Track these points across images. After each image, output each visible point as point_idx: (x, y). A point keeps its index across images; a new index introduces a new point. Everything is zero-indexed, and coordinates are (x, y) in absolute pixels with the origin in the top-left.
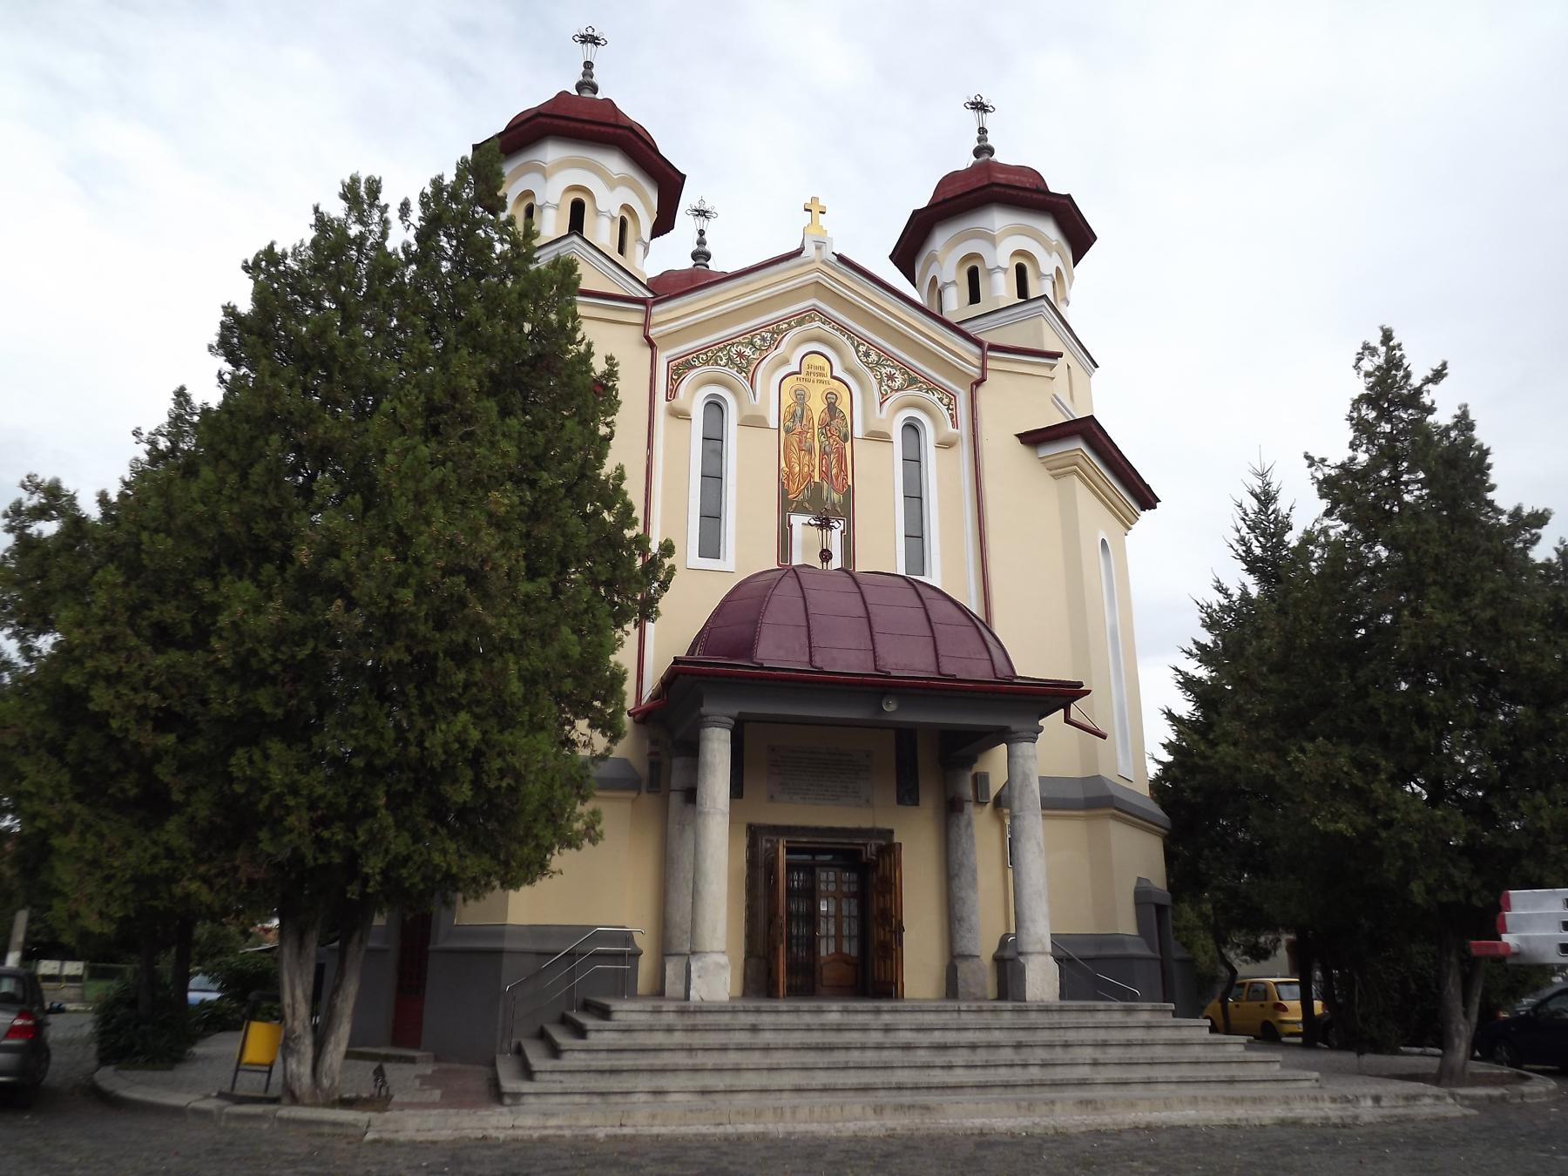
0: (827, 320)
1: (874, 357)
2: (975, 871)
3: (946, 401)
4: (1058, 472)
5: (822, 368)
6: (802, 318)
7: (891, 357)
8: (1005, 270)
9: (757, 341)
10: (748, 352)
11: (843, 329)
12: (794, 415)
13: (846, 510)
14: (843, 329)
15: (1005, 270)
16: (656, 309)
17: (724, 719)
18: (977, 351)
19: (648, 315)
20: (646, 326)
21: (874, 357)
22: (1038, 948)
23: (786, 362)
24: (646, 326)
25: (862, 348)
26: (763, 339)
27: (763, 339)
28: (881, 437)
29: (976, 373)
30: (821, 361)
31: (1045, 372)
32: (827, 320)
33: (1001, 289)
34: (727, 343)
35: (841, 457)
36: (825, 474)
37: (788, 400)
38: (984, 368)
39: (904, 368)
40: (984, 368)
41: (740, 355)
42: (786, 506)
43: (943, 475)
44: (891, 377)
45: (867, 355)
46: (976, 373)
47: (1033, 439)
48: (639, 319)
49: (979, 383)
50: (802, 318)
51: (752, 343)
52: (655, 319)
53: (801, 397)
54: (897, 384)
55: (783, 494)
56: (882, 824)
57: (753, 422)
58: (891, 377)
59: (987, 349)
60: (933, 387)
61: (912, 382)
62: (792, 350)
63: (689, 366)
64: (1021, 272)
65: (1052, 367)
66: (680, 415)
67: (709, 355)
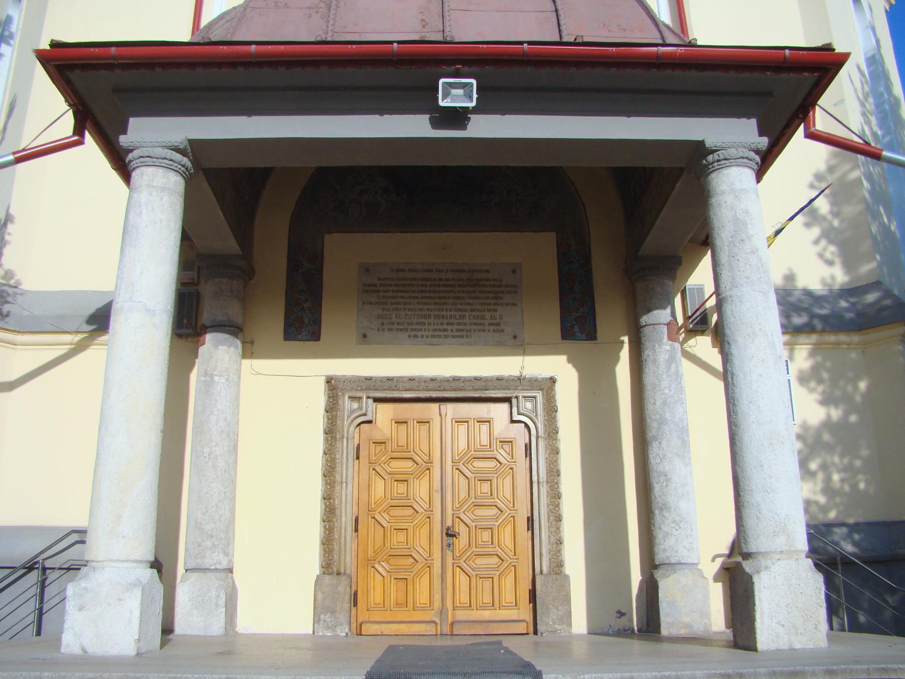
2: (683, 431)
17: (160, 152)
22: (780, 543)
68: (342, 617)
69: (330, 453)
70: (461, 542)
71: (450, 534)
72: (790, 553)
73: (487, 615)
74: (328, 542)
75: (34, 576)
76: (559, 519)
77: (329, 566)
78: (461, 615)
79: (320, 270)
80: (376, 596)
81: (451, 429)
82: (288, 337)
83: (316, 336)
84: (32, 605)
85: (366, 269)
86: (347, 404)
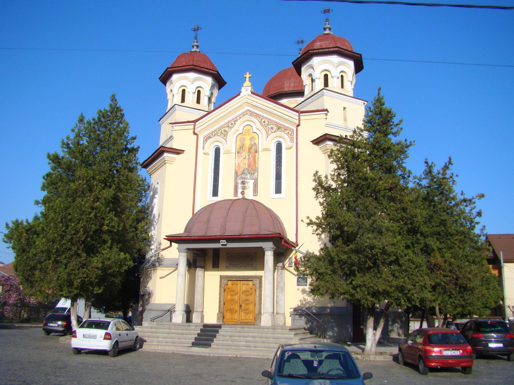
0: (252, 113)
1: (267, 122)
3: (290, 133)
5: (250, 130)
6: (244, 114)
7: (272, 121)
8: (319, 78)
9: (230, 125)
10: (227, 129)
11: (257, 116)
12: (240, 147)
14: (257, 116)
15: (319, 78)
16: (197, 123)
18: (298, 114)
19: (195, 126)
20: (194, 129)
21: (267, 122)
23: (238, 130)
24: (194, 129)
25: (263, 120)
26: (232, 124)
27: (232, 124)
28: (267, 150)
30: (249, 127)
32: (252, 113)
33: (319, 84)
34: (222, 127)
35: (254, 158)
36: (249, 165)
37: (238, 143)
38: (299, 120)
39: (276, 124)
40: (299, 120)
41: (225, 131)
44: (272, 128)
45: (264, 122)
46: (297, 122)
48: (192, 127)
49: (298, 125)
50: (244, 114)
51: (228, 126)
52: (196, 127)
53: (243, 141)
54: (273, 131)
55: (236, 173)
57: (227, 152)
58: (272, 128)
59: (300, 112)
60: (286, 128)
61: (279, 128)
62: (239, 127)
63: (210, 138)
64: (326, 76)
65: (326, 115)
68: (222, 320)
69: (220, 290)
70: (243, 308)
71: (241, 306)
72: (267, 313)
73: (246, 321)
74: (219, 307)
75: (169, 312)
76: (261, 304)
77: (219, 311)
78: (242, 321)
79: (219, 254)
80: (228, 317)
81: (242, 287)
82: (213, 267)
83: (218, 267)
84: (170, 317)
85: (227, 253)
86: (223, 281)
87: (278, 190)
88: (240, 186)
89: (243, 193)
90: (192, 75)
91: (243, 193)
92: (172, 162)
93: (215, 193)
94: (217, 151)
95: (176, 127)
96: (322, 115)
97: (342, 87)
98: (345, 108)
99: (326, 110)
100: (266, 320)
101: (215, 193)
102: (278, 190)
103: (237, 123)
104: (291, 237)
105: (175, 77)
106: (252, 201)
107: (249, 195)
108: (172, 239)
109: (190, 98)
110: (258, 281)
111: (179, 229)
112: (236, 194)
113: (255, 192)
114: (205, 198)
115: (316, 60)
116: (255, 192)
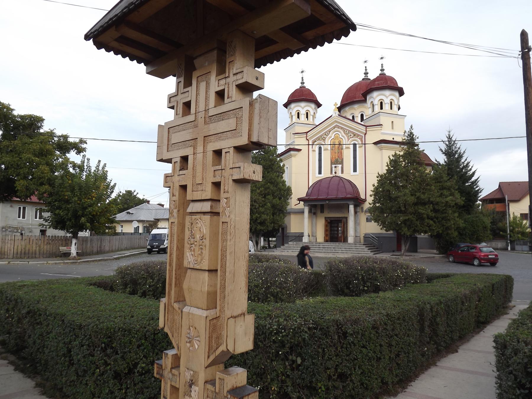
0: (339, 127)
4: (381, 149)
10: (325, 136)
11: (342, 128)
13: (342, 163)
14: (342, 128)
20: (306, 137)
24: (306, 137)
29: (365, 132)
31: (380, 128)
32: (339, 127)
39: (353, 133)
42: (332, 163)
43: (360, 151)
47: (376, 143)
49: (365, 134)
56: (346, 216)
57: (325, 150)
60: (359, 135)
61: (355, 135)
62: (332, 135)
64: (381, 103)
66: (314, 151)
67: (318, 139)
87: (355, 170)
88: (333, 169)
89: (335, 173)
90: (303, 104)
91: (335, 173)
92: (295, 155)
93: (320, 173)
94: (320, 149)
95: (296, 136)
96: (378, 128)
97: (391, 109)
98: (392, 122)
99: (382, 125)
100: (351, 240)
101: (320, 173)
102: (355, 170)
103: (331, 132)
104: (363, 196)
105: (293, 105)
106: (341, 178)
107: (339, 174)
108: (300, 200)
109: (303, 117)
110: (345, 220)
111: (303, 195)
112: (331, 173)
113: (342, 172)
114: (315, 177)
115: (375, 94)
116: (342, 172)
